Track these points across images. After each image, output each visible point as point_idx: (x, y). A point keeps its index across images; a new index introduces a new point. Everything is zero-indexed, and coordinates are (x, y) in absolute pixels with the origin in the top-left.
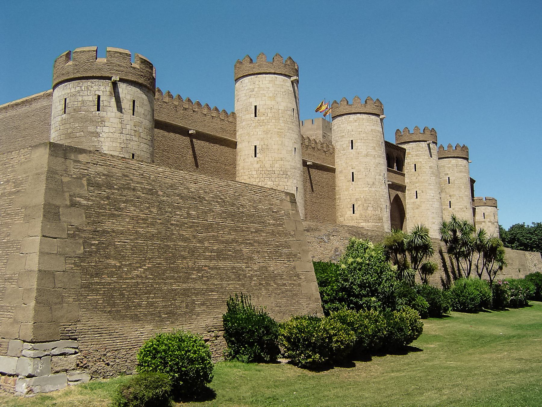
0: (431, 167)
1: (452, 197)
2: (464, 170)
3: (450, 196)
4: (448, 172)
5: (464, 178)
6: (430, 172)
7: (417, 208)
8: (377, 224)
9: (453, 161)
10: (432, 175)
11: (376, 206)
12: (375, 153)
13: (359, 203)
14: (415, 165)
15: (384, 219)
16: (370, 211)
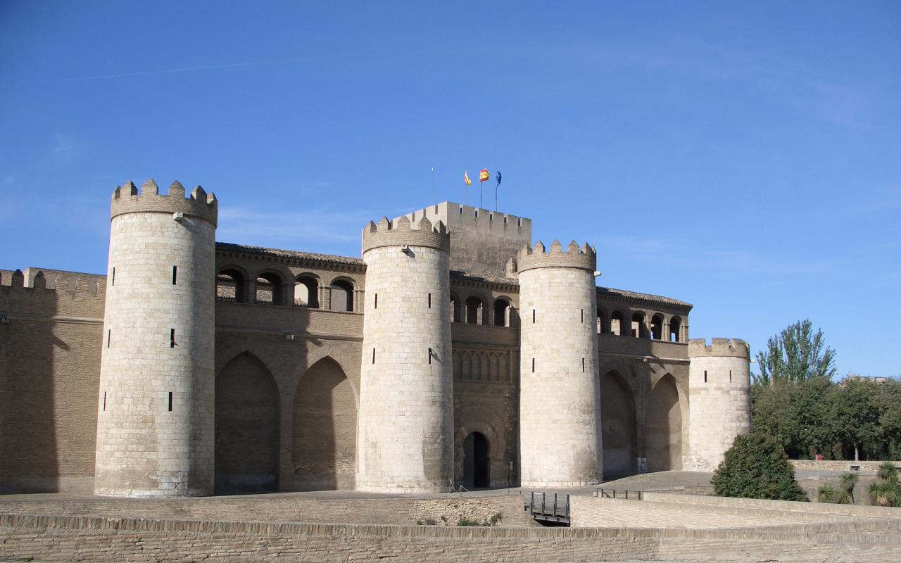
0: (405, 299)
1: (537, 352)
2: (566, 293)
3: (534, 348)
4: (534, 300)
5: (566, 310)
6: (402, 310)
7: (373, 384)
8: (138, 431)
9: (543, 275)
10: (406, 315)
11: (140, 395)
12: (148, 290)
13: (112, 389)
14: (376, 295)
15: (158, 420)
16: (127, 406)
